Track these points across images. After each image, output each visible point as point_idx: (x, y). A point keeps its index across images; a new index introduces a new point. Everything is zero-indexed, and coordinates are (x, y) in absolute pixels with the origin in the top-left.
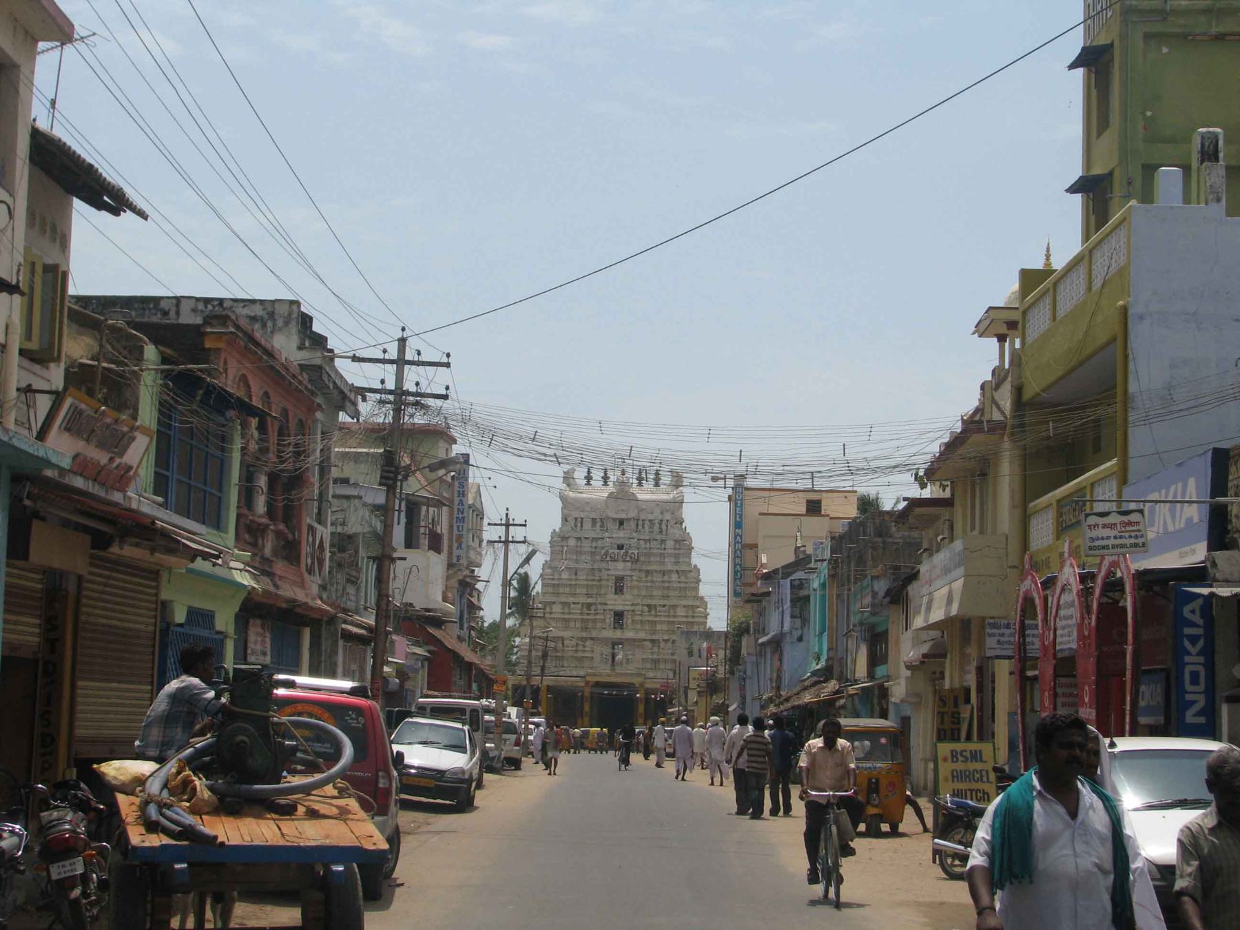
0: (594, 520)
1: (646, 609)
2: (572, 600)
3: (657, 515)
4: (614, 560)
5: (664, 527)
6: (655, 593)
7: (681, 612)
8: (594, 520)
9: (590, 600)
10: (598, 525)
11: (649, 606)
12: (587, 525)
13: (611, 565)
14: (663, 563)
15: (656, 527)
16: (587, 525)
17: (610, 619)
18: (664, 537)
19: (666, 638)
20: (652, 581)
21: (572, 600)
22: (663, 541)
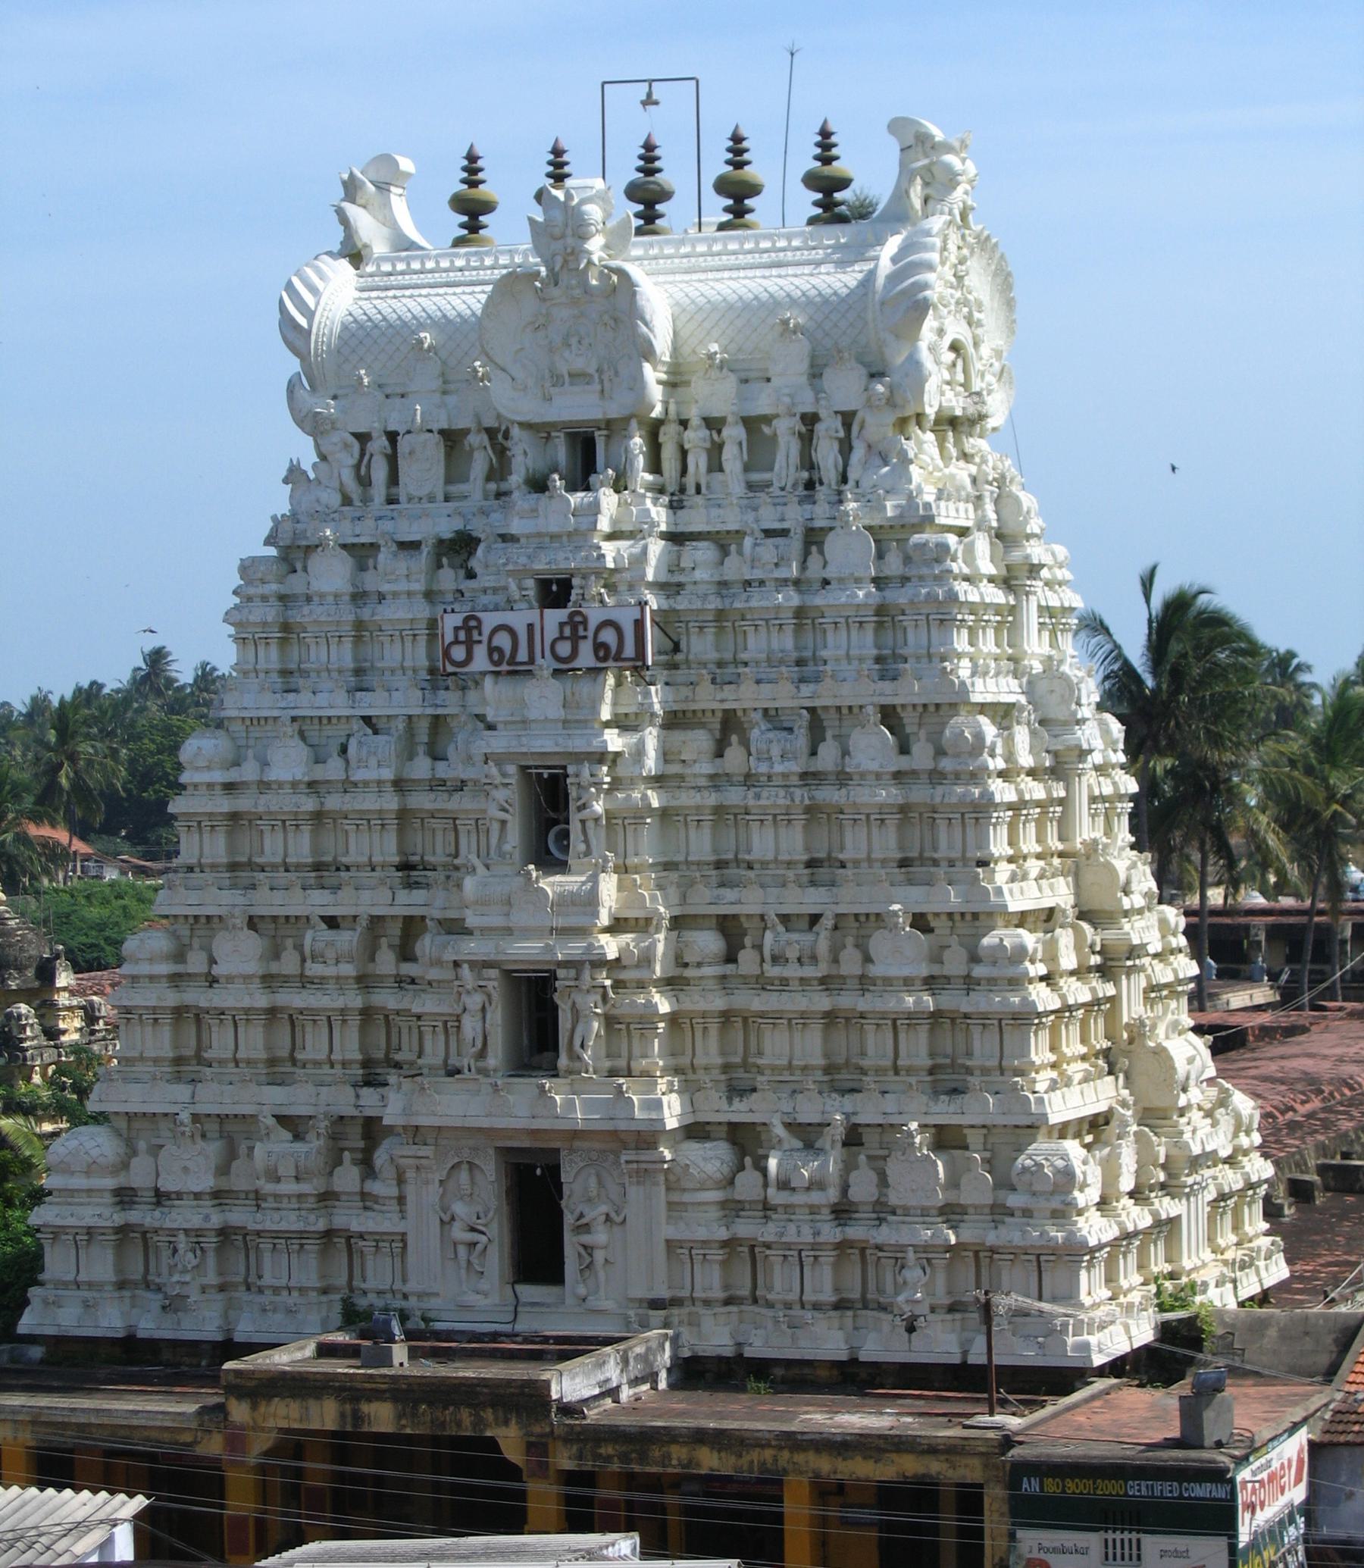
0: (452, 438)
1: (708, 942)
2: (319, 903)
3: (782, 394)
4: (512, 667)
5: (827, 455)
6: (762, 843)
7: (899, 954)
8: (452, 438)
9: (410, 902)
10: (479, 465)
11: (730, 929)
12: (423, 469)
13: (494, 697)
14: (806, 667)
15: (788, 449)
16: (423, 469)
17: (488, 1021)
18: (820, 514)
19: (808, 1112)
20: (749, 780)
21: (319, 903)
22: (814, 538)
